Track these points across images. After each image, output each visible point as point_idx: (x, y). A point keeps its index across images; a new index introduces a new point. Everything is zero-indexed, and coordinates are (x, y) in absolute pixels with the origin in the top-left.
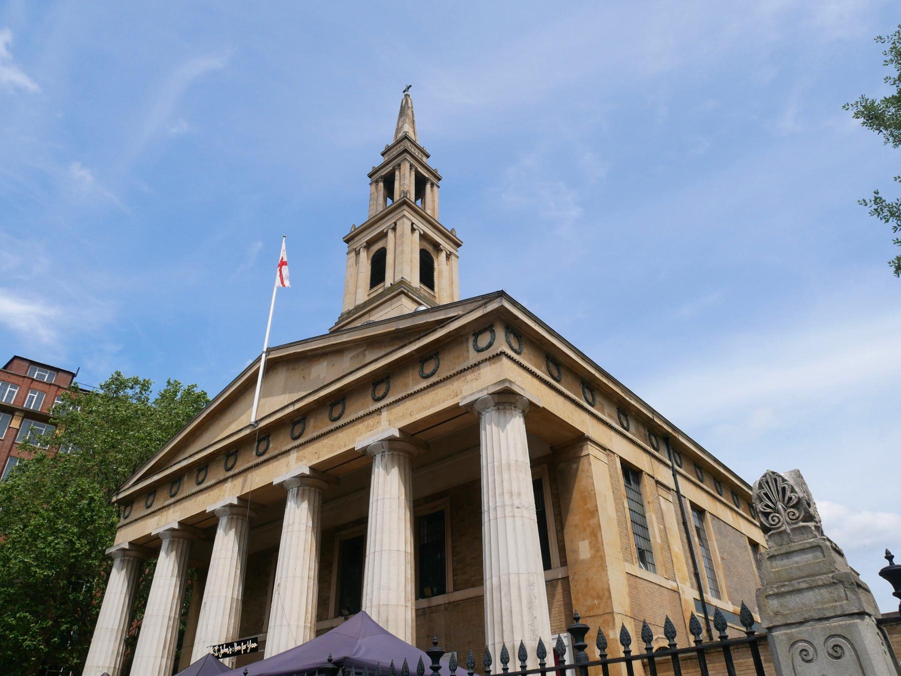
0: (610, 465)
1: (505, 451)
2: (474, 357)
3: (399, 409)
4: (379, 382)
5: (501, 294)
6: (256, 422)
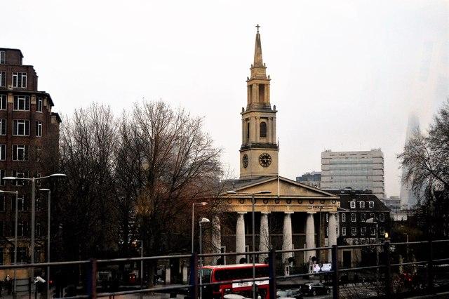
2: (331, 204)
4: (312, 201)
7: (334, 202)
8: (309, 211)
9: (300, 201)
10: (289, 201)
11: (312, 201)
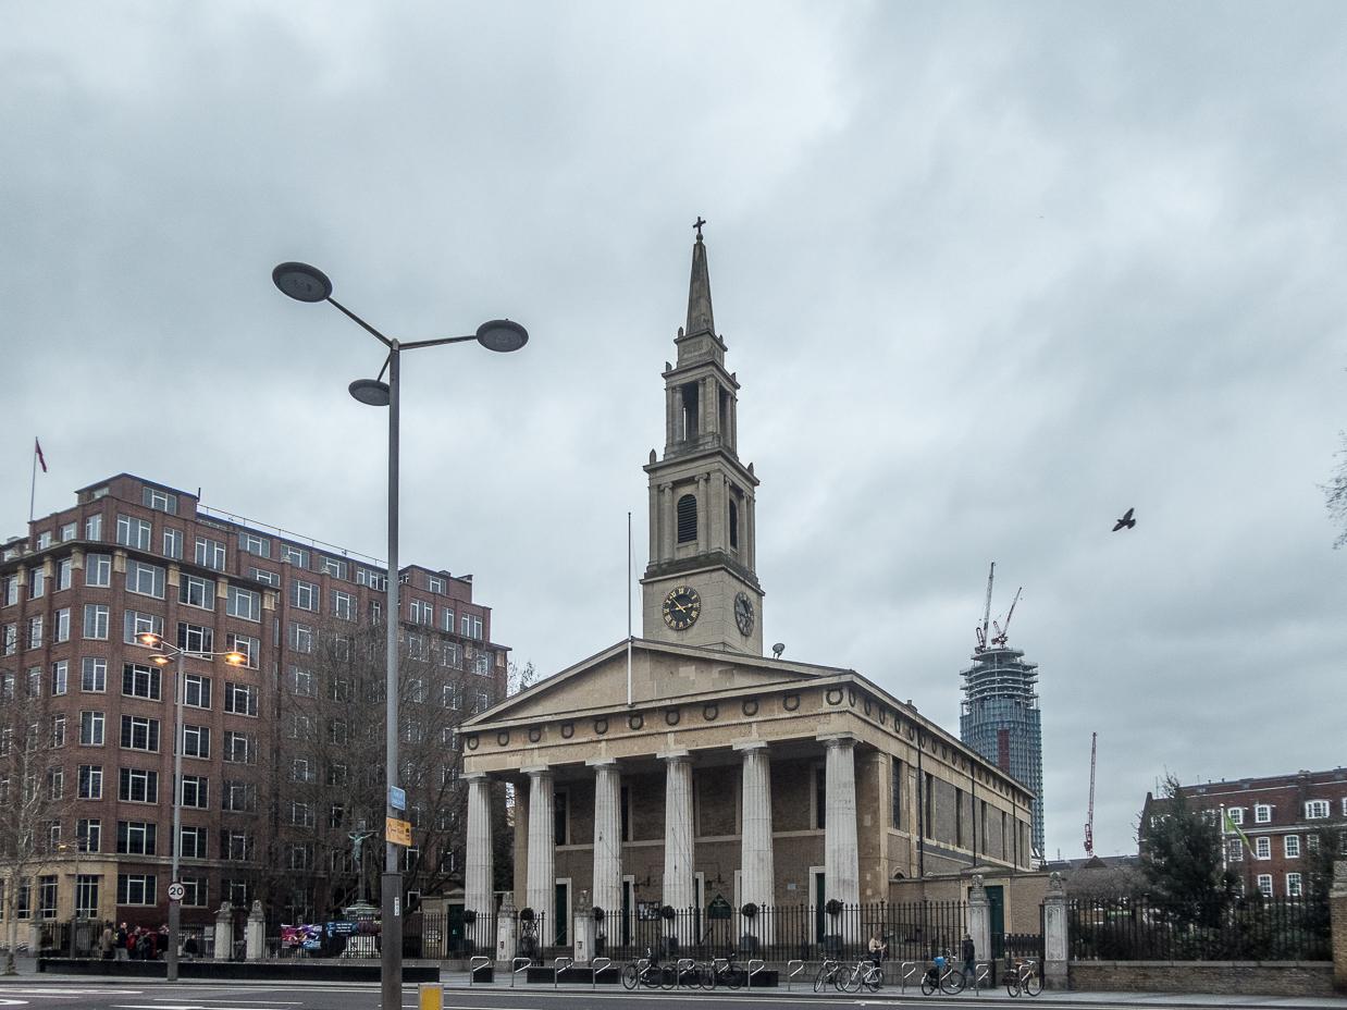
0: (889, 762)
1: (839, 767)
2: (826, 707)
3: (767, 727)
4: (750, 702)
5: (852, 672)
6: (633, 704)
7: (835, 697)
8: (739, 743)
9: (711, 707)
10: (672, 712)
11: (750, 702)
